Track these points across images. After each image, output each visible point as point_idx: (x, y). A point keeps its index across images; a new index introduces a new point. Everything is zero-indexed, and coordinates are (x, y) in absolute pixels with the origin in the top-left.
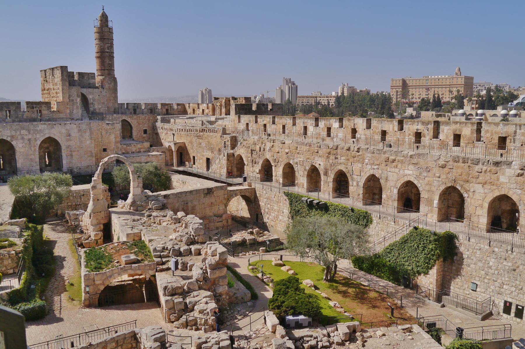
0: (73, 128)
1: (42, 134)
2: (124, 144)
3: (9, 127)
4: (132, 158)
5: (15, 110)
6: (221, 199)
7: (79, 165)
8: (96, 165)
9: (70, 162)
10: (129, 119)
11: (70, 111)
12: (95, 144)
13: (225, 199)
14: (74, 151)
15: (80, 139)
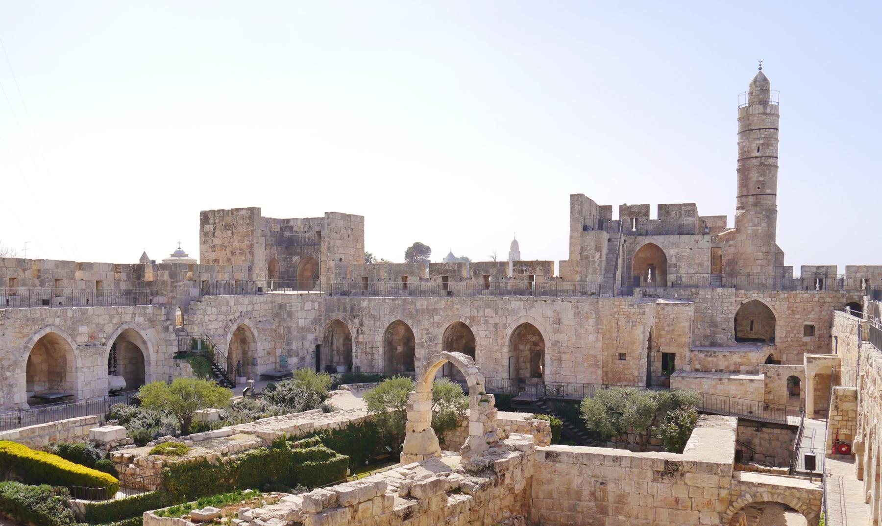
0: (566, 308)
1: (515, 317)
2: (701, 352)
3: (469, 303)
4: (680, 379)
5: (496, 276)
6: (707, 497)
7: (572, 381)
8: (603, 384)
9: (557, 373)
10: (769, 299)
11: (581, 278)
12: (604, 343)
13: (721, 500)
14: (565, 353)
15: (576, 331)
